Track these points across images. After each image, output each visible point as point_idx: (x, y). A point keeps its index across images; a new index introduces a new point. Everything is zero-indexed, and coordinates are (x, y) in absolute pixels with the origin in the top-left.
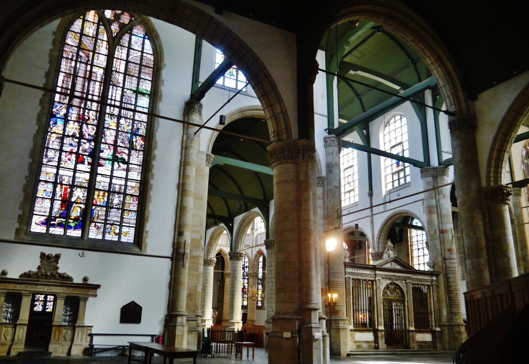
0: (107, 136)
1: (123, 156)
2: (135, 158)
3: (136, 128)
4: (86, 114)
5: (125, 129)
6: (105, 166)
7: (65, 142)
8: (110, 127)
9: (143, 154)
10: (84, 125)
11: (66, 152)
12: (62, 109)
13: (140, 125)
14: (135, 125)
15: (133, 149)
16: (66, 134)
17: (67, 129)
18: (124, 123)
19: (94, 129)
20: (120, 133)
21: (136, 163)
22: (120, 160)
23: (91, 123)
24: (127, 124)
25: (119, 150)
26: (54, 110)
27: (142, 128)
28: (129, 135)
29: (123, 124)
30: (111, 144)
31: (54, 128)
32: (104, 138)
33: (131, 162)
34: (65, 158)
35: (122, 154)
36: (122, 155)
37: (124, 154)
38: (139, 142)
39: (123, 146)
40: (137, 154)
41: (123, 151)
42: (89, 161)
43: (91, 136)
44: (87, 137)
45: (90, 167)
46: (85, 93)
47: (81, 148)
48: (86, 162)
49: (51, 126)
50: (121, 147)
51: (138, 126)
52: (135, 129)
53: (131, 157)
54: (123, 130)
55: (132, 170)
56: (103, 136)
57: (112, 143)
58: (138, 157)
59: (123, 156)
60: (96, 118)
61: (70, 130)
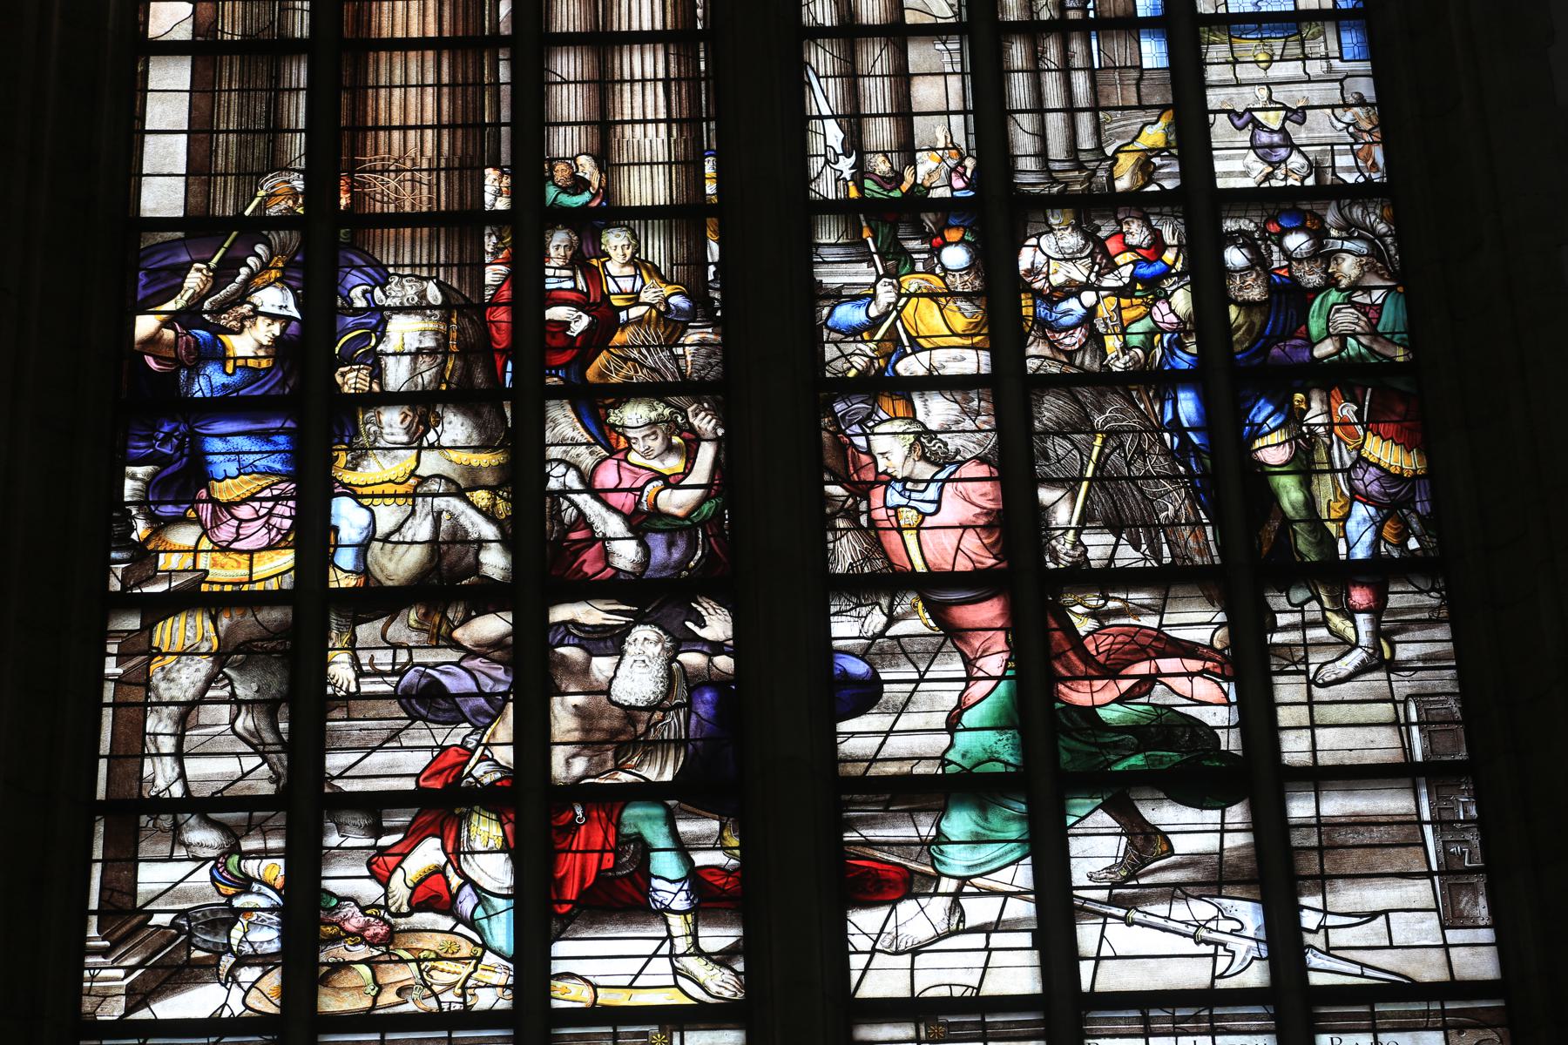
0: (888, 480)
1: (1159, 695)
2: (1345, 690)
3: (1255, 294)
4: (557, 278)
5: (1112, 343)
6: (947, 885)
7: (341, 670)
8: (911, 366)
9: (1449, 600)
10: (563, 423)
11: (373, 807)
12: (243, 296)
13: (1297, 242)
14: (1235, 257)
15: (1291, 573)
16: (342, 579)
17: (348, 518)
18: (1079, 273)
19: (693, 441)
20: (1051, 410)
21: (1380, 746)
22: (1137, 761)
23: (642, 376)
24: (1109, 281)
25: (1084, 626)
26: (145, 325)
27: (1348, 267)
28: (1187, 406)
29: (1072, 290)
30: (963, 565)
31: (185, 536)
32: (852, 515)
33: (1295, 748)
34: (370, 891)
35: (1142, 668)
36: (1148, 682)
37: (1168, 665)
38: (1343, 456)
39: (1127, 556)
40: (1362, 619)
41: (1151, 621)
42: (701, 859)
43: (672, 526)
44: (626, 554)
45: (717, 938)
46: (496, 41)
47: (563, 718)
48: (669, 891)
49: (141, 529)
50: (1111, 578)
51: (1277, 259)
52: (1246, 306)
53: (1288, 689)
54: (1088, 361)
55: (1352, 861)
56: (835, 490)
57: (975, 552)
58: (1392, 666)
59: (1159, 695)
60: (696, 291)
61: (387, 517)
